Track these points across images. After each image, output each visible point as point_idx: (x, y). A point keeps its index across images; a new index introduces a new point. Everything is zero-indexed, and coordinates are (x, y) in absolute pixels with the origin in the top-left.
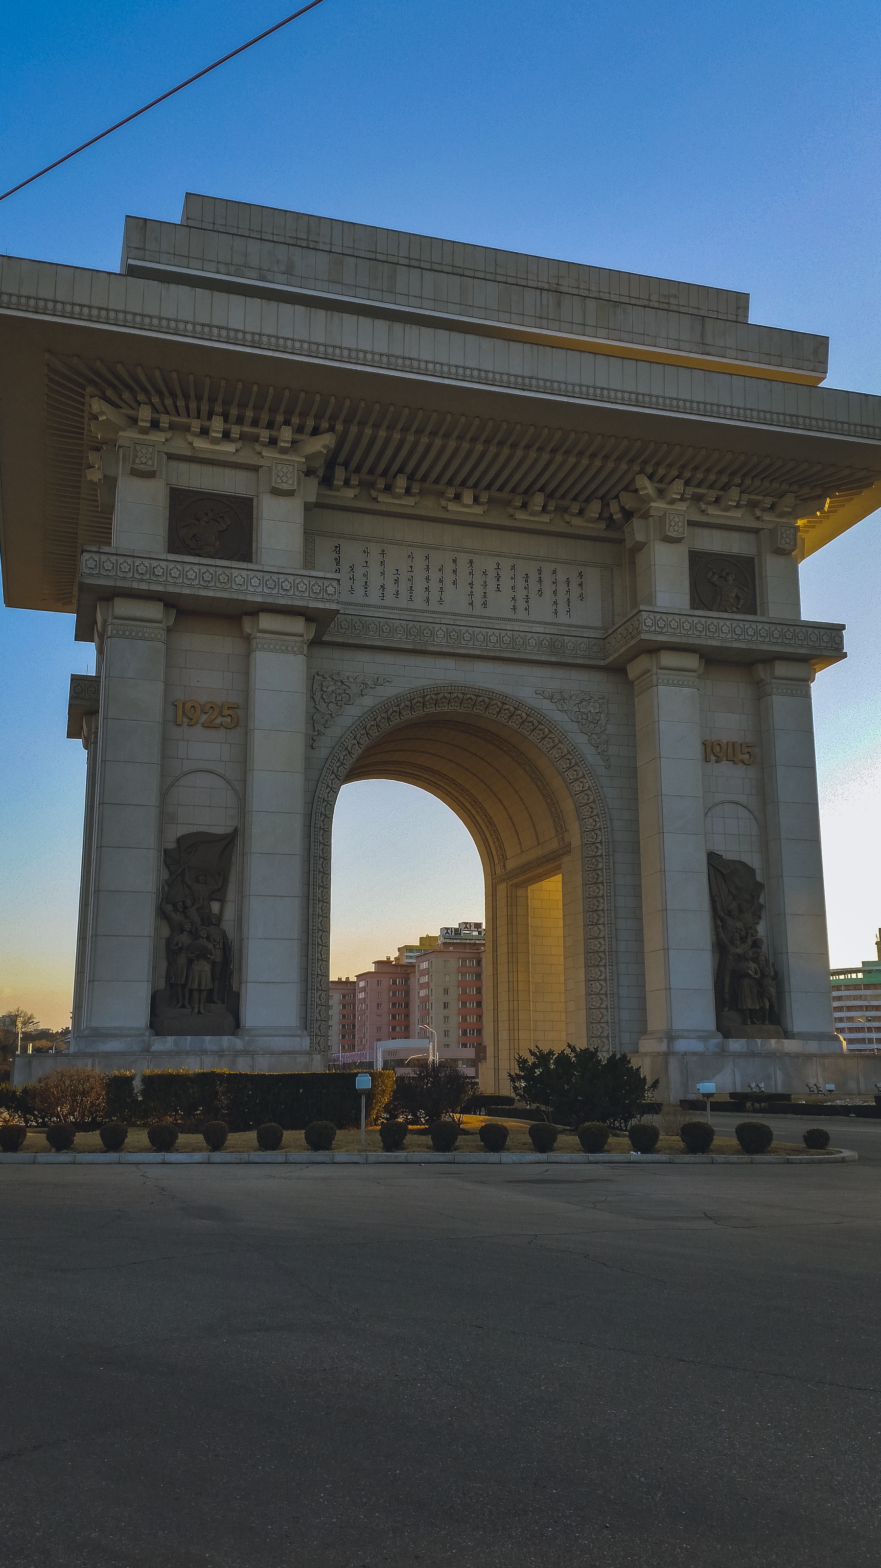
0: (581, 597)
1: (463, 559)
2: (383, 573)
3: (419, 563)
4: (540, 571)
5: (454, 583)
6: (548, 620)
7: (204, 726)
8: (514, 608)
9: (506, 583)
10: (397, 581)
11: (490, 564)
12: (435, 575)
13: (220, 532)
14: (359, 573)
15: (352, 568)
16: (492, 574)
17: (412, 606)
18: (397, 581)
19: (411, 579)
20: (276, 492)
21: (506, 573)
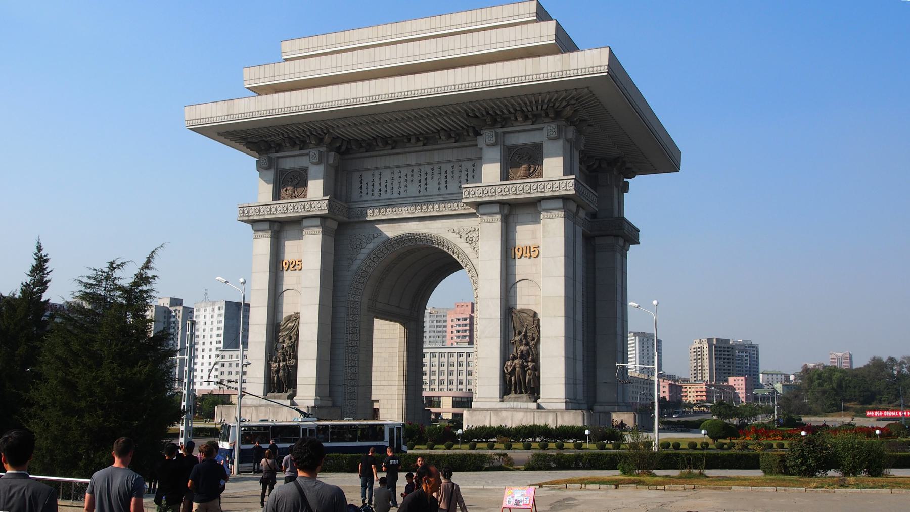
0: (473, 176)
1: (416, 169)
2: (380, 184)
3: (396, 175)
4: (453, 167)
5: (412, 181)
6: (457, 192)
7: (291, 270)
8: (439, 189)
9: (436, 177)
10: (386, 186)
11: (428, 169)
12: (403, 180)
13: (296, 184)
14: (370, 184)
15: (367, 184)
16: (430, 172)
17: (393, 197)
18: (386, 186)
19: (392, 184)
20: (313, 163)
21: (436, 171)
